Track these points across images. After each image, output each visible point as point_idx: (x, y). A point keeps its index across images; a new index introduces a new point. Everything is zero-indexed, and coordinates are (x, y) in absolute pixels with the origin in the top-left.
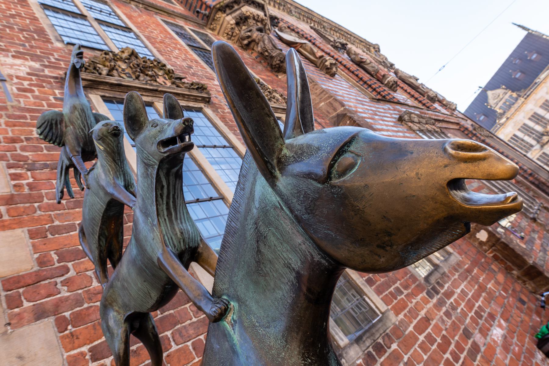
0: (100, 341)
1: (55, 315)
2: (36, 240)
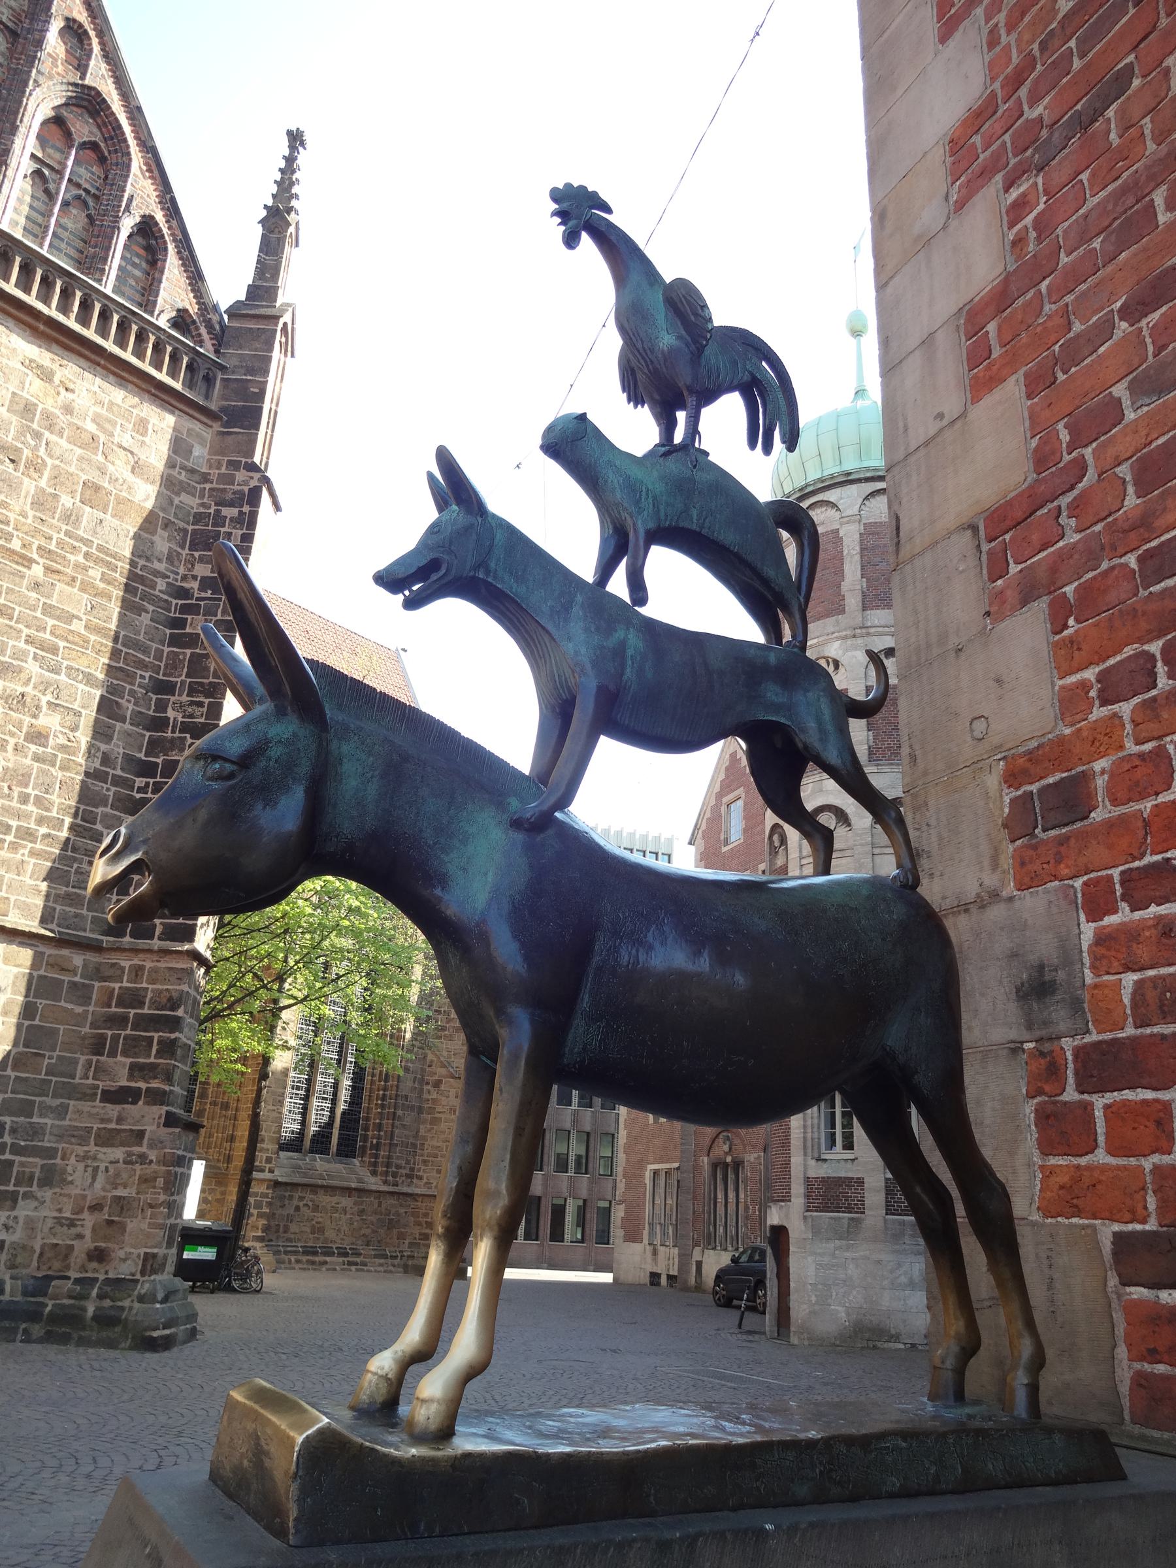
0: (1118, 658)
1: (1050, 593)
2: (1036, 400)
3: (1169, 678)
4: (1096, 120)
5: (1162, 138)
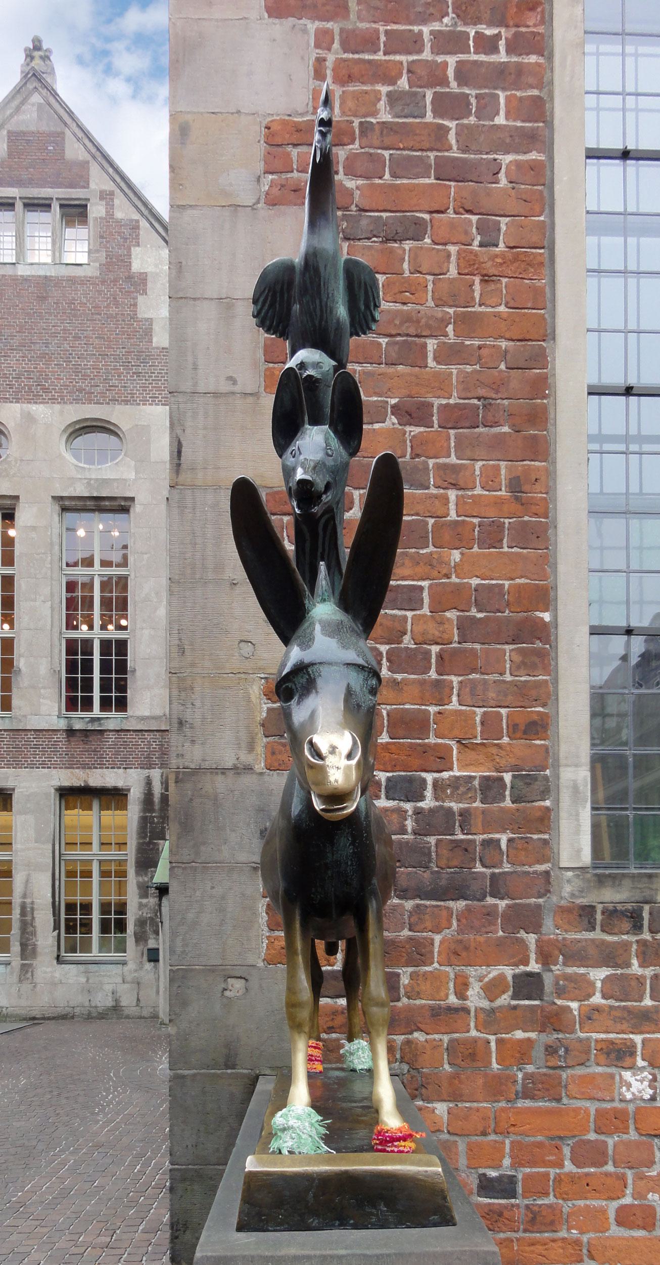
3: (389, 670)
4: (395, 241)
5: (441, 303)
